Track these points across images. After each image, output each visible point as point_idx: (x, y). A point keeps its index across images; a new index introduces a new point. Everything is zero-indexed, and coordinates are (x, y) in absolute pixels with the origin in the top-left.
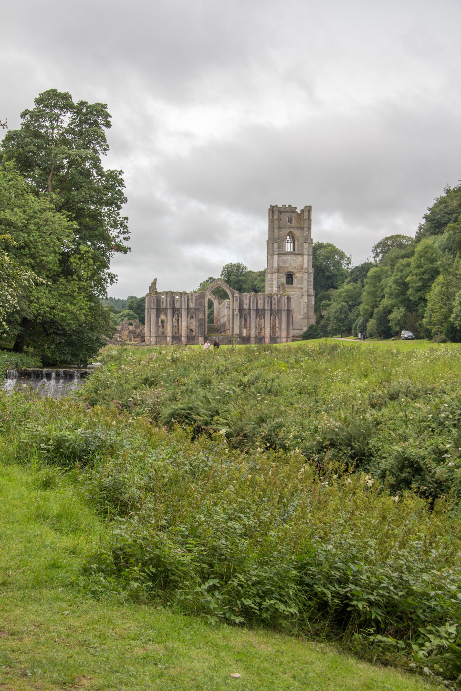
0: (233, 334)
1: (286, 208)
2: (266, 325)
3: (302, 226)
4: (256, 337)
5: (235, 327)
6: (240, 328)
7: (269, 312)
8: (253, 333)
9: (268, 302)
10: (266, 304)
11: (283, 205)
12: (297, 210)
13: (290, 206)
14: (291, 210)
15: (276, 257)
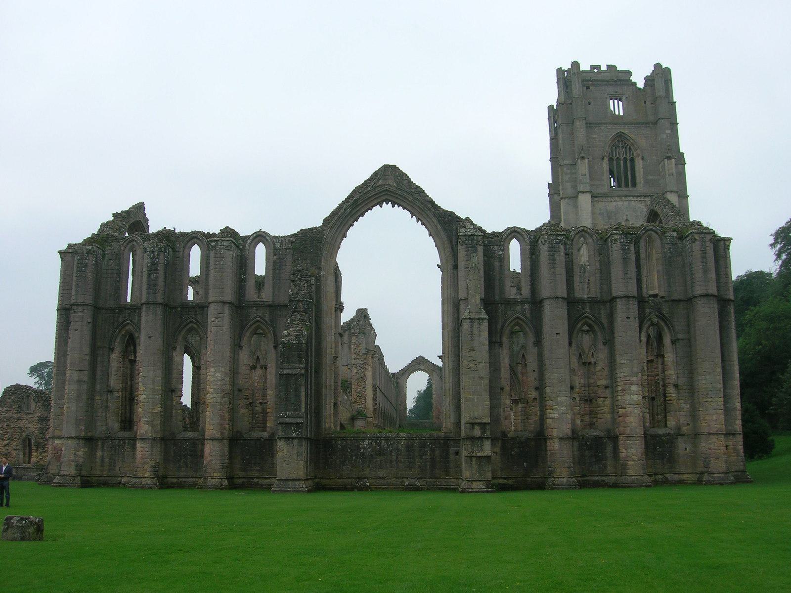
0: (458, 424)
1: (600, 72)
2: (622, 372)
3: (651, 118)
4: (574, 436)
5: (465, 380)
6: (494, 391)
7: (634, 306)
8: (561, 416)
9: (625, 260)
10: (617, 271)
11: (593, 67)
12: (633, 79)
13: (611, 68)
14: (615, 80)
15: (585, 200)
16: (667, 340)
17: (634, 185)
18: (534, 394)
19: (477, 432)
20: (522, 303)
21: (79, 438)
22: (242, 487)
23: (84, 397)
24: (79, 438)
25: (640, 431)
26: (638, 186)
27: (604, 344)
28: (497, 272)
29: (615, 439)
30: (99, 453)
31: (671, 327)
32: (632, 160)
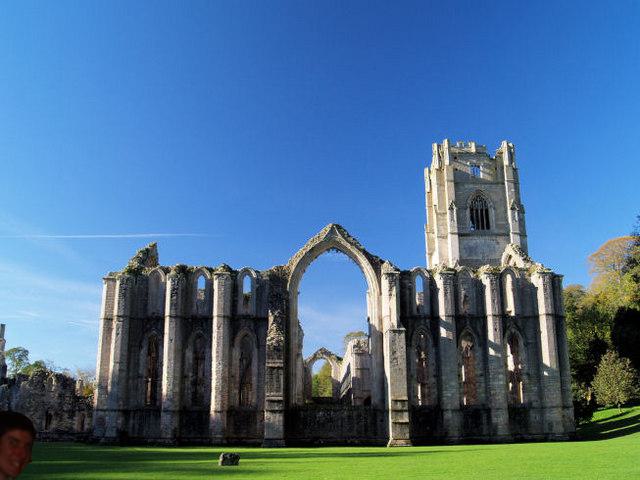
16: (521, 343)
17: (488, 228)
18: (433, 380)
19: (399, 406)
20: (425, 318)
21: (119, 410)
22: (476, 429)
23: (123, 381)
24: (119, 410)
25: (506, 405)
26: (491, 228)
27: (480, 345)
28: (408, 296)
29: (488, 411)
30: (131, 421)
31: (525, 336)
32: (487, 211)
